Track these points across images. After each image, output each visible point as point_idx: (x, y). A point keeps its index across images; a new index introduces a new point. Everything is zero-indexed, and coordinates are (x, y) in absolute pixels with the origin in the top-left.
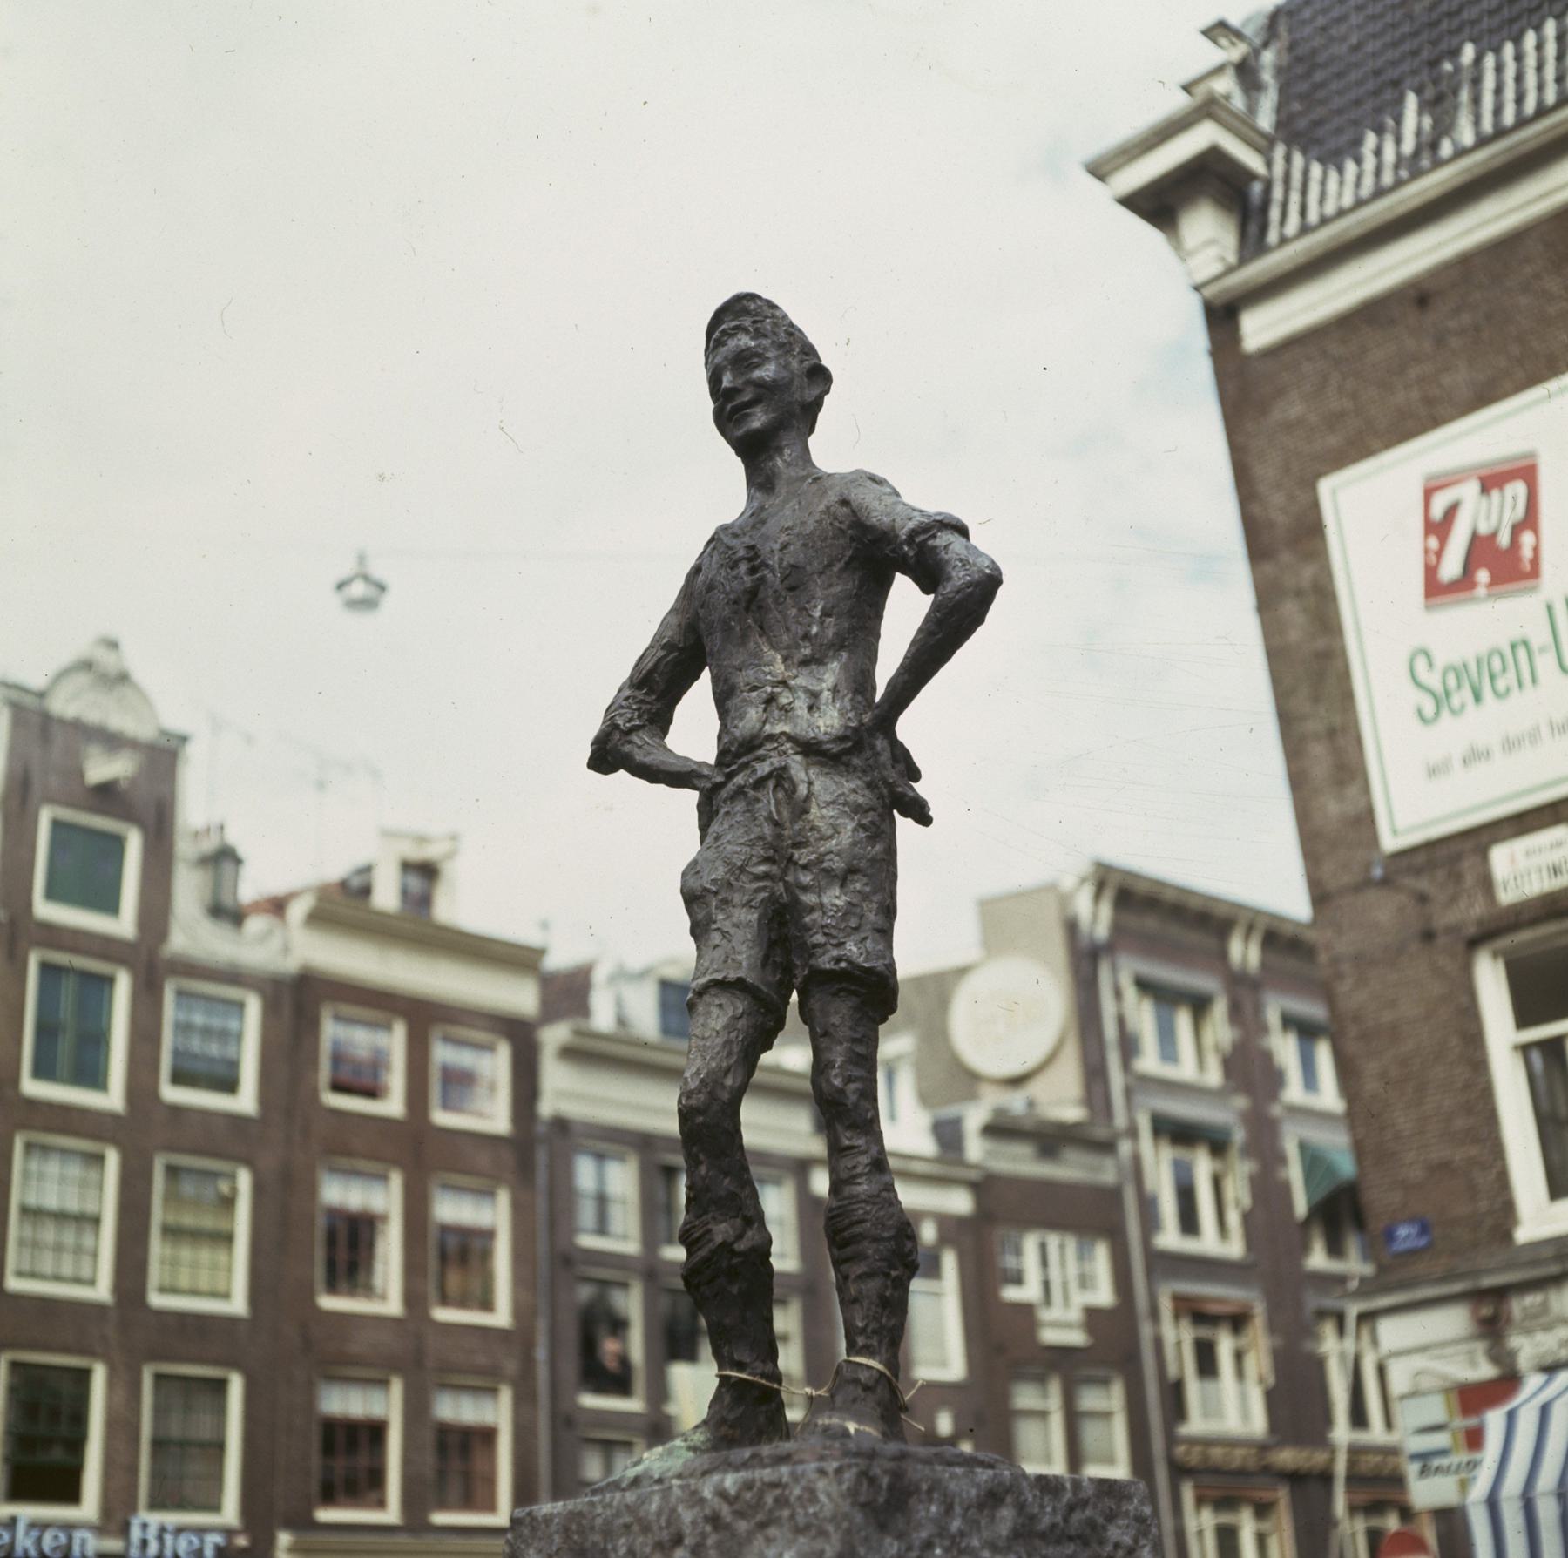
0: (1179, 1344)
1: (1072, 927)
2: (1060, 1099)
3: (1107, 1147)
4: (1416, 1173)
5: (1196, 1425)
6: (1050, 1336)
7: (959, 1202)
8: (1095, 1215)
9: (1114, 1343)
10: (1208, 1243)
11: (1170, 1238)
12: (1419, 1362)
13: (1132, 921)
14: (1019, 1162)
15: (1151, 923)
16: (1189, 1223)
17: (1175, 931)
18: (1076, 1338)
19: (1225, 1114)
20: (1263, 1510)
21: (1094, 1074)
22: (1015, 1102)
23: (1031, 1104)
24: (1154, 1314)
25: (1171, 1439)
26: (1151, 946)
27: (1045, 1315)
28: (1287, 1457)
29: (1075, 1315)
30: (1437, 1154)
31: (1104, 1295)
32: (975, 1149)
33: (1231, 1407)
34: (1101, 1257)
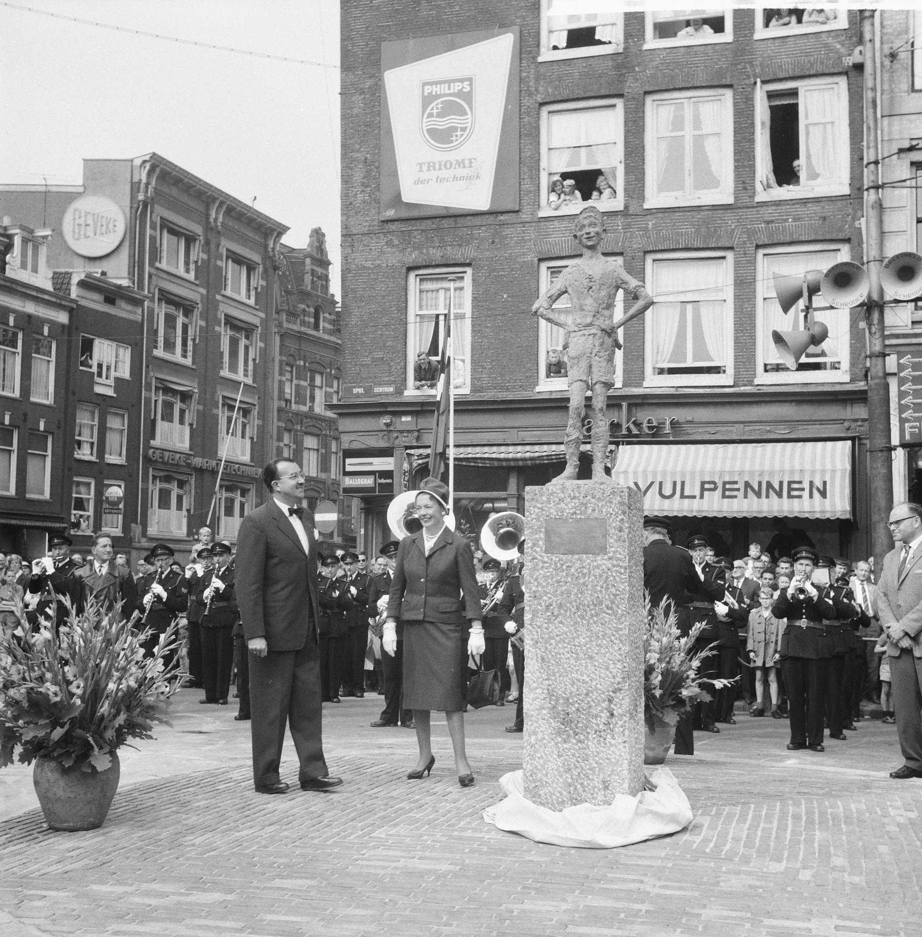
0: (156, 401)
1: (135, 187)
2: (118, 274)
3: (138, 302)
4: (368, 360)
5: (156, 442)
6: (98, 389)
7: (63, 318)
8: (129, 335)
9: (128, 397)
10: (177, 357)
11: (159, 352)
12: (352, 437)
13: (165, 189)
14: (94, 302)
15: (174, 191)
16: (169, 345)
17: (185, 198)
18: (110, 392)
19: (194, 295)
20: (181, 484)
21: (136, 265)
22: (96, 270)
23: (104, 274)
24: (148, 389)
25: (147, 447)
26: (173, 205)
27: (97, 379)
28: (198, 461)
29: (111, 382)
30: (380, 355)
31: (125, 372)
32: (74, 292)
33: (174, 436)
34: (126, 355)
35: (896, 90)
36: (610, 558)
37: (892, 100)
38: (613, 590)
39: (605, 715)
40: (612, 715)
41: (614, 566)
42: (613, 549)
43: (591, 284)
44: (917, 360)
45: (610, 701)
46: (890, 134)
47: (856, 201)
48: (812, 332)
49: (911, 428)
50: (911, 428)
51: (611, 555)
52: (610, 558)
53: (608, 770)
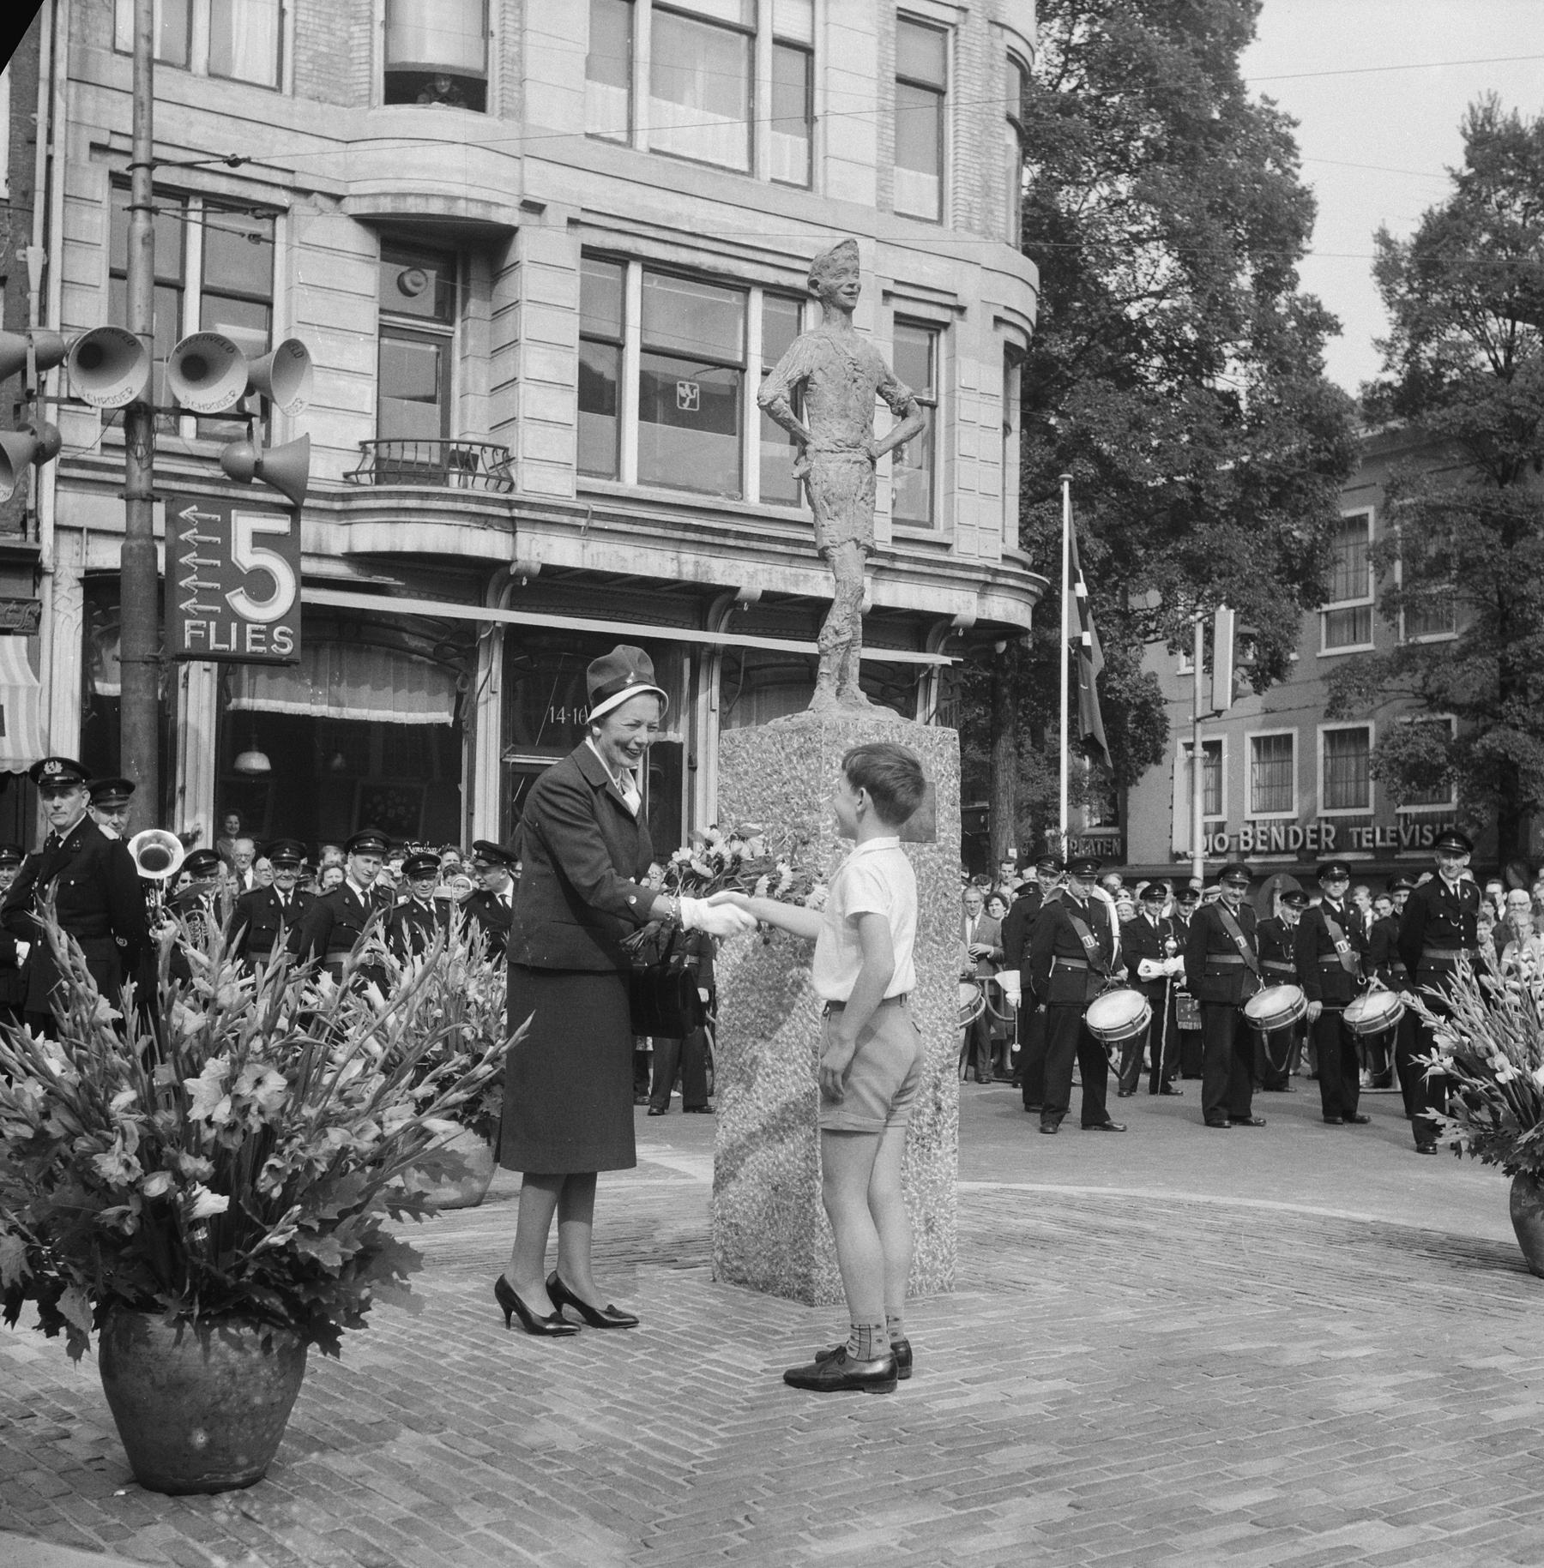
35: (92, 40)
36: (941, 850)
37: (84, 53)
38: (944, 902)
39: (930, 1110)
40: (939, 1109)
41: (945, 863)
42: (944, 835)
43: (856, 374)
44: (207, 516)
45: (936, 1087)
46: (78, 113)
47: (20, 214)
48: (40, 439)
49: (193, 628)
50: (193, 628)
51: (942, 843)
52: (941, 850)
53: (931, 1200)
